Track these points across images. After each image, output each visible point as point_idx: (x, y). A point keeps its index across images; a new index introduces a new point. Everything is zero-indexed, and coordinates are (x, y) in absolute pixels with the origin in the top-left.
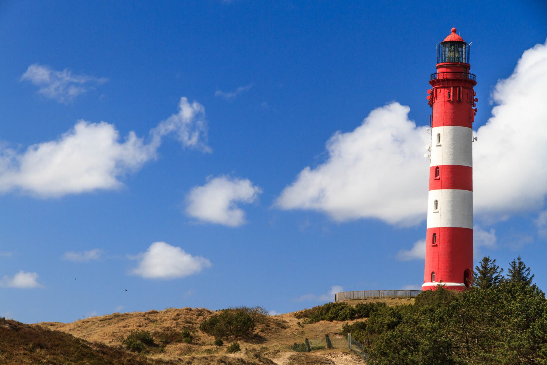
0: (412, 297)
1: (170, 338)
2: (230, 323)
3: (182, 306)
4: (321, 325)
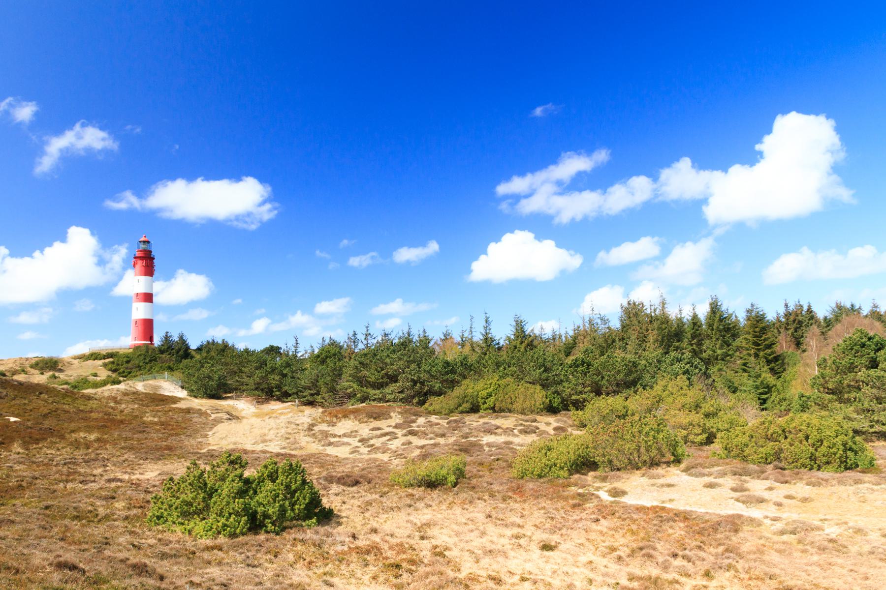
1: (14, 373)
2: (46, 364)
3: (17, 356)
4: (90, 362)
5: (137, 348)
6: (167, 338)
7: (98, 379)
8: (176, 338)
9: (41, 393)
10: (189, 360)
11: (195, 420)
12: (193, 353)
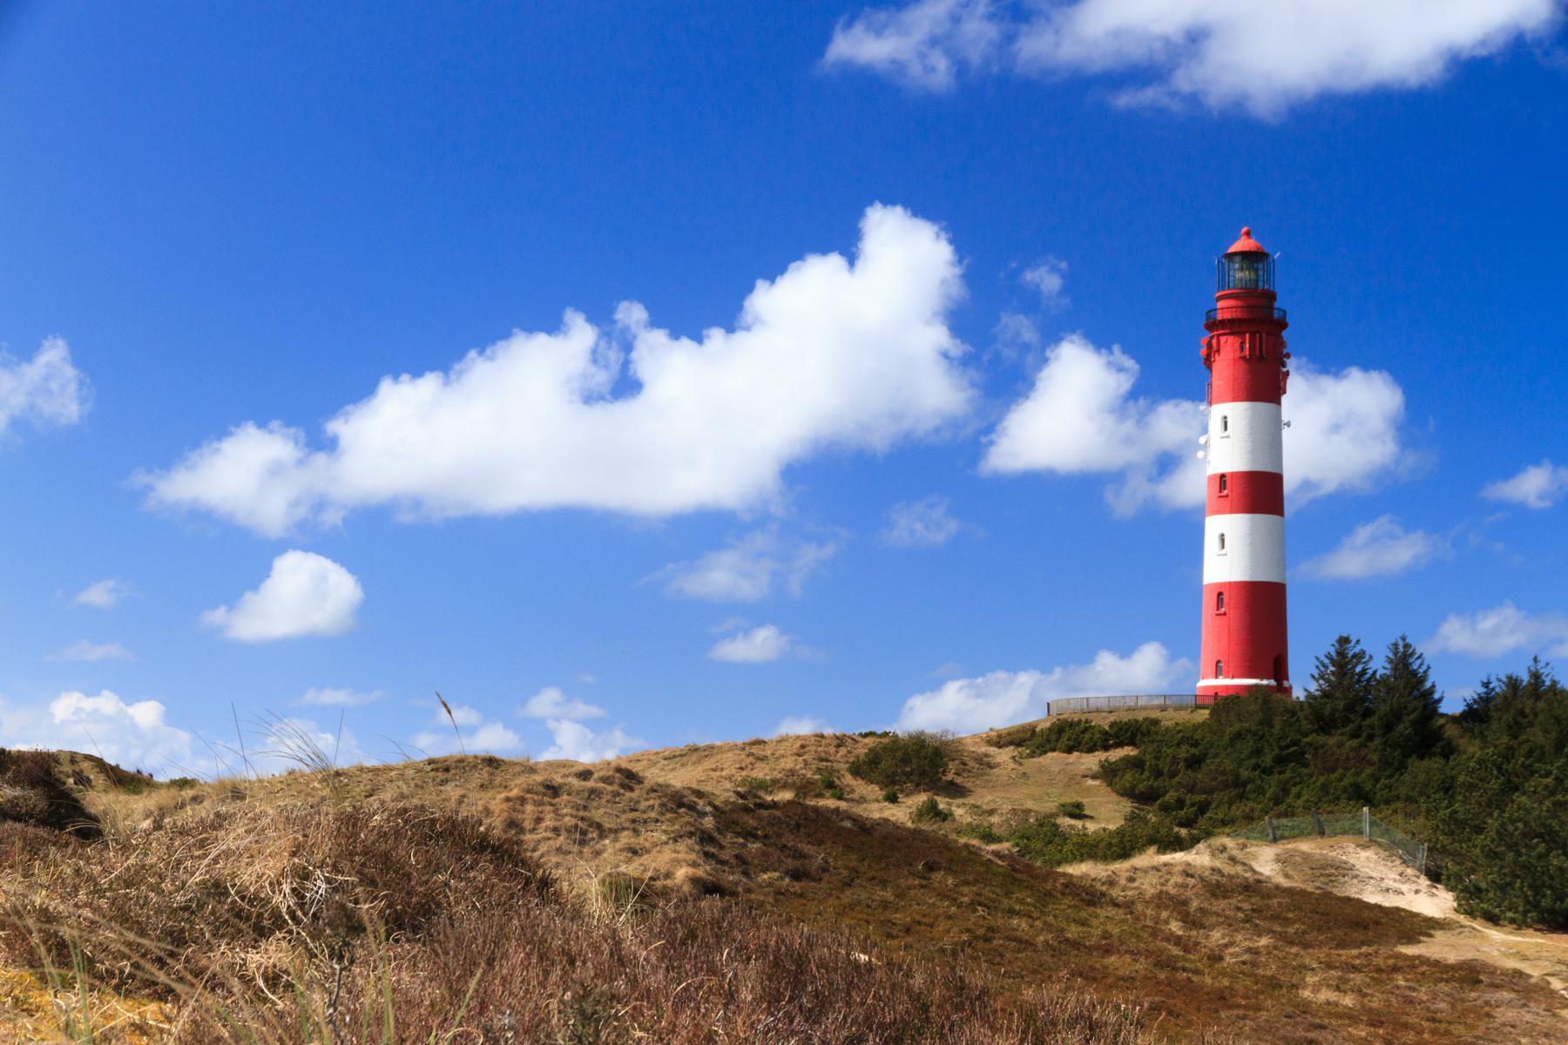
0: (1198, 707)
2: (906, 761)
4: (1053, 759)
5: (1224, 704)
6: (1344, 660)
7: (1091, 827)
8: (1379, 664)
9: (931, 867)
10: (1435, 763)
11: (1504, 1015)
12: (1451, 731)
